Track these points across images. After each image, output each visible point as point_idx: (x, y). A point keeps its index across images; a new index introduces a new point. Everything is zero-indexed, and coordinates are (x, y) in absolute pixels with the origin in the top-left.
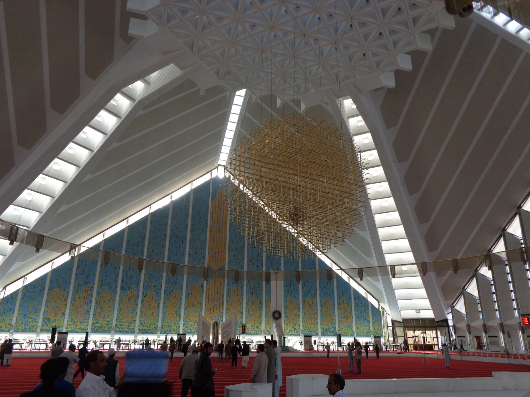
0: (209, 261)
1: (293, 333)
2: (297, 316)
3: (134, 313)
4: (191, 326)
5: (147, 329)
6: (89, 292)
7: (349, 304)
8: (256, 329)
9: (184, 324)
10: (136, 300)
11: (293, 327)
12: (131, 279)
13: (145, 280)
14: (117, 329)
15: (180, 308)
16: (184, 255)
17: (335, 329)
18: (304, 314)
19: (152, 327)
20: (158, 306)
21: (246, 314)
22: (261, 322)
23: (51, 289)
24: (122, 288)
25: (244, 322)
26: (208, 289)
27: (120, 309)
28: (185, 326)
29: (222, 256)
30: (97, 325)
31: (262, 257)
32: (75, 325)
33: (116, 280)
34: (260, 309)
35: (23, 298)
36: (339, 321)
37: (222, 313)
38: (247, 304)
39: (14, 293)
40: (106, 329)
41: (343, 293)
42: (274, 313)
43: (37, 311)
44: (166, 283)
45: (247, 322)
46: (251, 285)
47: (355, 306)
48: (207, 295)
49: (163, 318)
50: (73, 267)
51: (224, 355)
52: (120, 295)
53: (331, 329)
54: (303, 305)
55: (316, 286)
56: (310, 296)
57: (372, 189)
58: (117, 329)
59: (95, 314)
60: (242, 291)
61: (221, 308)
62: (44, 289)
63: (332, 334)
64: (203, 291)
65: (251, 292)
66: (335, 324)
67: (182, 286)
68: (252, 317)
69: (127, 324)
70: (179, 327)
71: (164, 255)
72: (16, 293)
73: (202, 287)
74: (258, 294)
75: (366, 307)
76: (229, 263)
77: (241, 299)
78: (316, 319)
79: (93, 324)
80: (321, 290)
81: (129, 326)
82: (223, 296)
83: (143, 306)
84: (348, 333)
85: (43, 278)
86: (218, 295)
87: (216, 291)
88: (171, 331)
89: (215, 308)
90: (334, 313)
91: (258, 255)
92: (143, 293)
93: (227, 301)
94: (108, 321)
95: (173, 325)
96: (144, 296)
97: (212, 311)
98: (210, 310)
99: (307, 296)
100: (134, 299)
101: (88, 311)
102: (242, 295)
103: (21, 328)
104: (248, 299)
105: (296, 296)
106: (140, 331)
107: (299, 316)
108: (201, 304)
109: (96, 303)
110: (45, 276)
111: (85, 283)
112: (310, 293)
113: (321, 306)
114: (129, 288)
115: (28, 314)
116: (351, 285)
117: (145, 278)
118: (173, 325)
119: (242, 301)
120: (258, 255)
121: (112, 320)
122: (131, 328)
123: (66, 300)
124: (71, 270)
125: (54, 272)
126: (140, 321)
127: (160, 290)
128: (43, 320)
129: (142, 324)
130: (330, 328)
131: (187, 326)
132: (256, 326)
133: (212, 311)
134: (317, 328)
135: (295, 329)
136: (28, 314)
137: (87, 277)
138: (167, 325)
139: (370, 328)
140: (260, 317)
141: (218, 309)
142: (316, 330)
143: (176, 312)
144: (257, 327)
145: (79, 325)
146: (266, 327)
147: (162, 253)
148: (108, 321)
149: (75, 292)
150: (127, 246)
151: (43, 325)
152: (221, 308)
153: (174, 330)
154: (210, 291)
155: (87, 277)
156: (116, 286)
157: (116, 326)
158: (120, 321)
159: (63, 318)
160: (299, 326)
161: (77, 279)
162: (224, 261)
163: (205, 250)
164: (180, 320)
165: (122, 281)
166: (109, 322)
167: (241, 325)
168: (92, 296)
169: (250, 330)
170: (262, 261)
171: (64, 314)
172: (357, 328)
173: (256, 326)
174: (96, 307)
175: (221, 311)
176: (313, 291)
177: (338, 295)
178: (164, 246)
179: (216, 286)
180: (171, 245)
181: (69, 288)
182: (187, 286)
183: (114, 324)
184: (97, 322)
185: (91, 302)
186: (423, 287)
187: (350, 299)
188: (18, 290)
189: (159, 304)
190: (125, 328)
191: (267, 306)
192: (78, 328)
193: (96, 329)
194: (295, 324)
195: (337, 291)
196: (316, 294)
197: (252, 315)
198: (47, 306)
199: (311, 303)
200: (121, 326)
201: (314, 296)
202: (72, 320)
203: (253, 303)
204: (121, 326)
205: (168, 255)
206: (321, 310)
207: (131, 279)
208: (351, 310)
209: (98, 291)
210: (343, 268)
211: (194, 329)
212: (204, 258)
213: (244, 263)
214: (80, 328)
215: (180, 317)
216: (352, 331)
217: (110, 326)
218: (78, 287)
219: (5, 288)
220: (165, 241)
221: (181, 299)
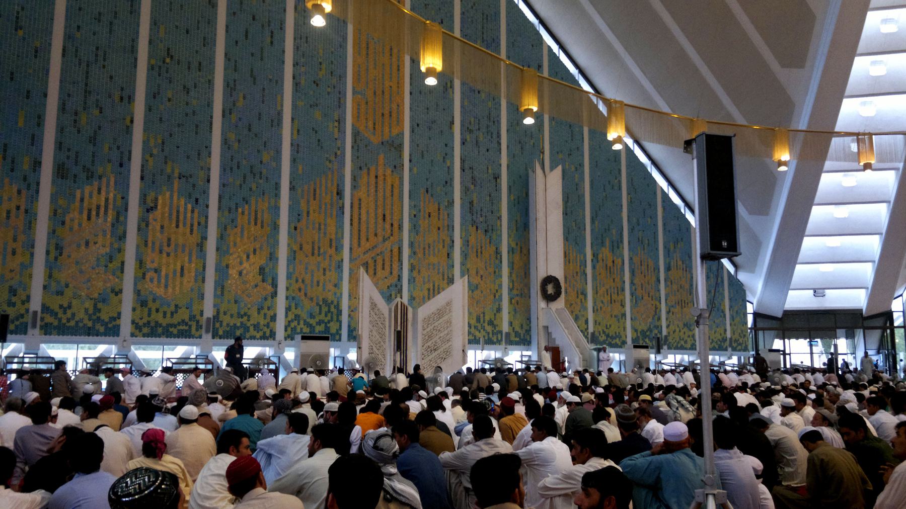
0: (357, 117)
2: (581, 296)
3: (116, 264)
4: (312, 316)
5: (164, 322)
8: (489, 328)
12: (93, 140)
14: (49, 319)
16: (278, 82)
17: (661, 333)
19: (184, 315)
20: (201, 246)
24: (61, 171)
26: (357, 204)
28: (291, 316)
29: (394, 106)
31: (499, 122)
33: (35, 140)
36: (668, 312)
37: (400, 278)
38: (465, 256)
41: (676, 243)
44: (223, 169)
46: (471, 203)
48: (356, 221)
51: (529, 387)
52: (54, 199)
54: (594, 267)
55: (621, 219)
58: (49, 319)
65: (473, 223)
66: (659, 319)
67: (277, 186)
70: (274, 318)
71: (212, 71)
73: (340, 194)
74: (490, 230)
76: (412, 131)
77: (448, 241)
81: (97, 310)
82: (400, 227)
86: (388, 226)
87: (380, 211)
88: (247, 329)
91: (489, 118)
93: (411, 245)
95: (254, 312)
99: (603, 244)
104: (466, 243)
108: (339, 249)
113: (632, 272)
114: (90, 176)
117: (145, 143)
119: (452, 246)
120: (489, 118)
122: (105, 317)
126: (138, 292)
127: (205, 192)
129: (144, 304)
130: (650, 330)
134: (624, 329)
138: (234, 310)
139: (725, 330)
142: (622, 333)
144: (491, 323)
146: (511, 324)
154: (363, 211)
156: (37, 164)
157: (45, 308)
158: (60, 293)
162: (400, 121)
163: (342, 77)
164: (274, 295)
165: (59, 146)
170: (499, 136)
175: (395, 272)
176: (614, 232)
177: (665, 247)
178: (209, 42)
179: (380, 194)
180: (232, 43)
183: (35, 305)
189: (204, 238)
190: (81, 315)
195: (664, 234)
196: (622, 242)
199: (610, 264)
200: (64, 310)
203: (479, 253)
204: (64, 310)
205: (226, 76)
211: (319, 323)
213: (452, 134)
215: (275, 285)
220: (211, 22)
221: (276, 227)
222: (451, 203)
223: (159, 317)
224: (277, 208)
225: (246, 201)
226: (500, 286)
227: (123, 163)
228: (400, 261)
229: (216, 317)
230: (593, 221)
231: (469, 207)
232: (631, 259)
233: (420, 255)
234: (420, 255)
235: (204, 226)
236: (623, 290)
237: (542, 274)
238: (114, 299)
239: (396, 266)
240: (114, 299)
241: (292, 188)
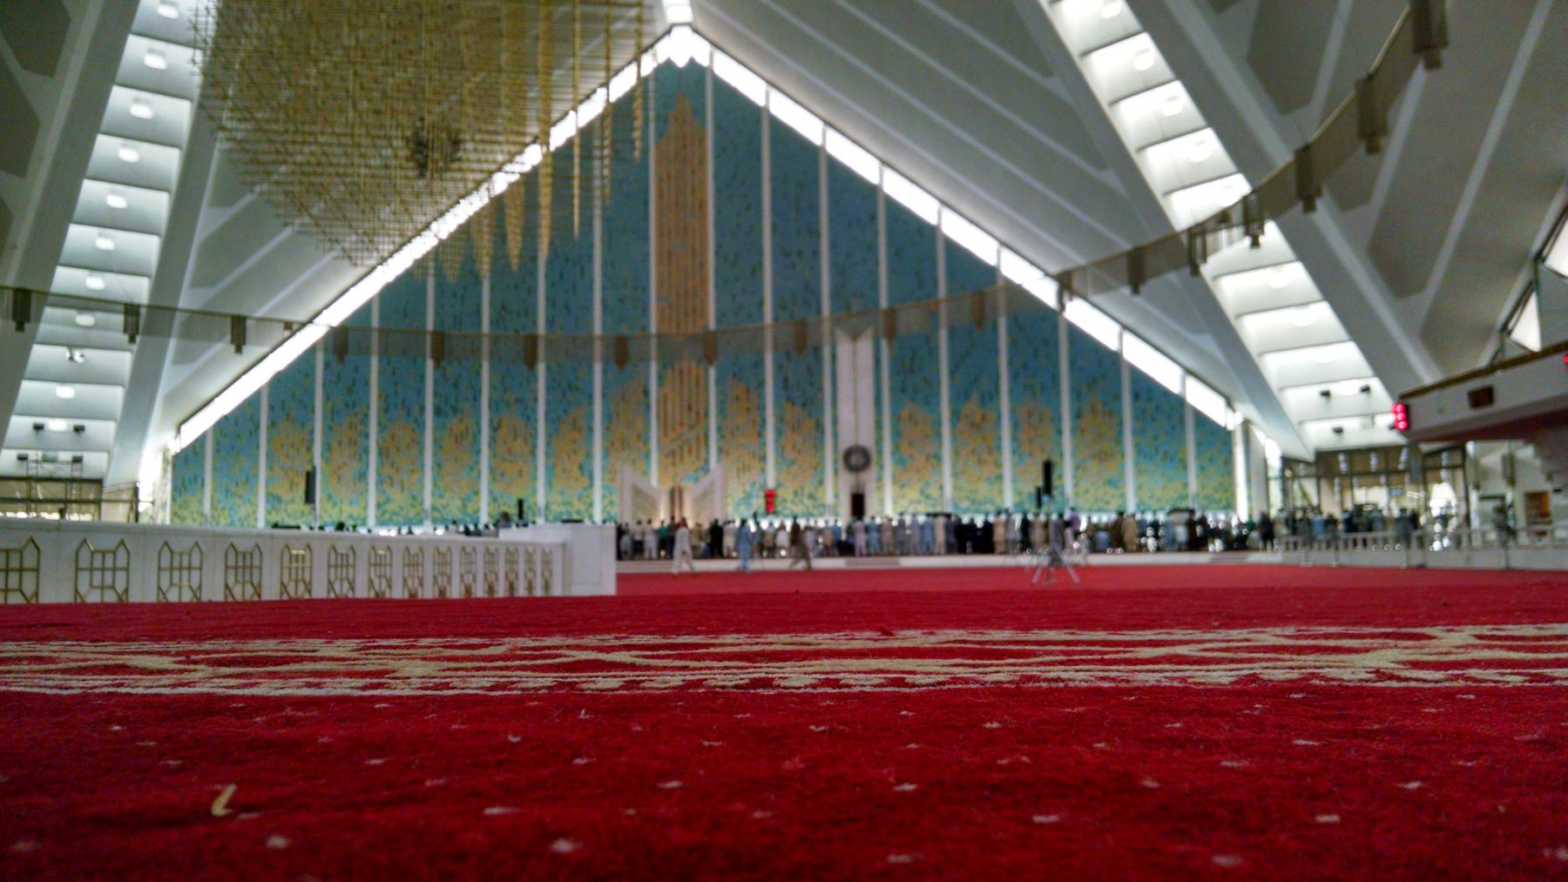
2: (933, 461)
3: (474, 474)
7: (1114, 414)
8: (808, 502)
9: (604, 497)
10: (476, 441)
11: (922, 492)
12: (456, 385)
13: (493, 387)
14: (436, 515)
15: (589, 455)
16: (589, 308)
18: (956, 453)
20: (533, 453)
21: (777, 463)
22: (821, 483)
23: (273, 424)
24: (438, 412)
25: (771, 484)
26: (663, 400)
27: (438, 466)
32: (337, 510)
33: (420, 392)
34: (819, 446)
35: (217, 450)
38: (779, 432)
39: (197, 440)
40: (412, 515)
41: (1092, 383)
43: (250, 480)
45: (779, 485)
46: (786, 380)
49: (549, 484)
50: (313, 367)
56: (975, 396)
57: (1131, 118)
58: (436, 515)
59: (380, 482)
60: (761, 396)
61: (703, 449)
62: (257, 426)
64: (648, 406)
67: (591, 396)
68: (795, 467)
69: (458, 502)
70: (591, 505)
73: (646, 393)
78: (998, 465)
79: (379, 506)
80: (1014, 376)
81: (465, 506)
82: (707, 414)
83: (494, 455)
84: (1108, 503)
85: (252, 403)
87: (685, 404)
92: (491, 421)
93: (719, 429)
94: (414, 498)
95: (575, 502)
96: (495, 428)
98: (672, 456)
101: (363, 476)
102: (762, 408)
104: (780, 419)
105: (931, 400)
107: (938, 458)
108: (646, 441)
109: (380, 453)
110: (256, 397)
111: (347, 405)
112: (975, 387)
114: (455, 410)
115: (233, 489)
118: (575, 502)
121: (421, 493)
125: (279, 380)
126: (491, 492)
127: (535, 411)
132: (806, 492)
135: (928, 497)
136: (233, 489)
137: (350, 390)
140: (818, 467)
143: (581, 467)
144: (811, 496)
147: (529, 312)
149: (328, 429)
150: (437, 300)
152: (703, 449)
155: (350, 390)
156: (422, 409)
157: (434, 508)
160: (941, 488)
161: (327, 397)
163: (646, 289)
164: (591, 486)
165: (435, 394)
166: (416, 499)
167: (762, 494)
168: (367, 435)
172: (1139, 488)
173: (806, 492)
174: (381, 464)
178: (532, 290)
180: (551, 285)
181: (312, 420)
184: (388, 501)
185: (366, 451)
188: (204, 435)
191: (835, 435)
193: (387, 516)
194: (927, 484)
197: (793, 462)
198: (270, 468)
200: (445, 507)
201: (992, 395)
202: (330, 497)
203: (796, 428)
209: (379, 424)
212: (645, 311)
215: (591, 477)
217: (418, 508)
218: (332, 414)
219: (179, 430)
221: (591, 429)
222: (762, 384)
224: (590, 415)
225: (566, 412)
226: (822, 459)
227: (476, 398)
229: (547, 507)
230: (952, 374)
231: (784, 384)
232: (1013, 411)
235: (535, 436)
236: (999, 448)
237: (846, 441)
241: (604, 395)
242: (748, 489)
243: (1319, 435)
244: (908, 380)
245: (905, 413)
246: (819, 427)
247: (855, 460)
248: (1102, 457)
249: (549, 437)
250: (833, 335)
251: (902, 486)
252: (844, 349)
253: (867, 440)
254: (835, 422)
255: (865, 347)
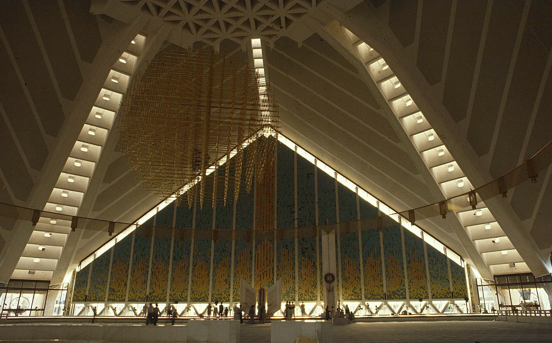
1: (353, 297)
3: (186, 282)
5: (198, 298)
6: (146, 264)
8: (312, 295)
9: (234, 292)
11: (353, 291)
12: (181, 249)
15: (229, 276)
16: (231, 222)
19: (203, 295)
23: (114, 262)
24: (174, 259)
27: (173, 279)
28: (235, 294)
30: (153, 294)
33: (169, 251)
34: (314, 273)
35: (93, 271)
38: (300, 268)
42: (326, 276)
47: (430, 263)
48: (256, 261)
50: (131, 241)
53: (399, 291)
54: (364, 266)
59: (151, 284)
62: (109, 263)
63: (401, 297)
64: (252, 258)
66: (404, 285)
67: (231, 253)
70: (229, 295)
72: (88, 267)
73: (251, 253)
75: (444, 264)
80: (386, 247)
81: (182, 295)
86: (268, 261)
89: (265, 273)
90: (403, 273)
92: (193, 262)
93: (277, 267)
94: (163, 291)
97: (262, 278)
100: (186, 268)
101: (146, 282)
103: (92, 298)
106: (192, 299)
111: (142, 255)
113: (387, 266)
116: (425, 240)
122: (184, 297)
123: (127, 272)
124: (130, 244)
126: (192, 289)
127: (210, 259)
128: (110, 291)
129: (193, 292)
131: (237, 294)
133: (262, 278)
141: (268, 276)
145: (138, 294)
148: (163, 291)
149: (134, 264)
151: (109, 295)
153: (224, 298)
159: (125, 288)
160: (361, 290)
161: (135, 252)
164: (230, 288)
165: (174, 252)
168: (148, 267)
169: (303, 296)
171: (126, 285)
172: (433, 289)
173: (310, 291)
177: (406, 253)
179: (265, 250)
182: (235, 254)
184: (154, 292)
185: (147, 273)
186: (494, 219)
187: (423, 256)
192: (137, 297)
194: (355, 288)
196: (380, 253)
202: (133, 290)
206: (386, 271)
207: (181, 249)
208: (425, 268)
209: (153, 263)
210: (399, 211)
214: (139, 297)
216: (426, 292)
221: (230, 266)
222: (294, 249)
223: (197, 296)
228: (273, 273)
233: (281, 270)
234: (281, 270)
238: (186, 291)
239: (271, 274)
240: (186, 291)
242: (288, 290)
243: (504, 269)
244: (346, 249)
245: (346, 261)
246: (314, 265)
247: (328, 278)
248: (418, 278)
249: (214, 269)
250: (320, 232)
251: (346, 289)
252: (324, 238)
253: (333, 271)
254: (321, 264)
255: (332, 236)
